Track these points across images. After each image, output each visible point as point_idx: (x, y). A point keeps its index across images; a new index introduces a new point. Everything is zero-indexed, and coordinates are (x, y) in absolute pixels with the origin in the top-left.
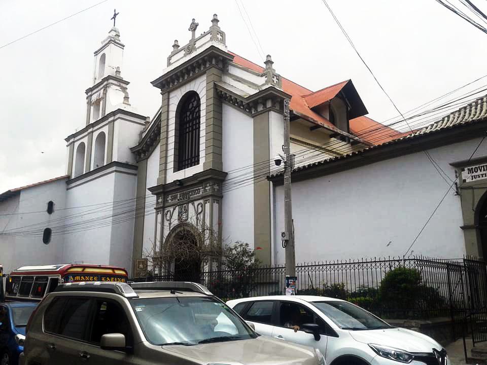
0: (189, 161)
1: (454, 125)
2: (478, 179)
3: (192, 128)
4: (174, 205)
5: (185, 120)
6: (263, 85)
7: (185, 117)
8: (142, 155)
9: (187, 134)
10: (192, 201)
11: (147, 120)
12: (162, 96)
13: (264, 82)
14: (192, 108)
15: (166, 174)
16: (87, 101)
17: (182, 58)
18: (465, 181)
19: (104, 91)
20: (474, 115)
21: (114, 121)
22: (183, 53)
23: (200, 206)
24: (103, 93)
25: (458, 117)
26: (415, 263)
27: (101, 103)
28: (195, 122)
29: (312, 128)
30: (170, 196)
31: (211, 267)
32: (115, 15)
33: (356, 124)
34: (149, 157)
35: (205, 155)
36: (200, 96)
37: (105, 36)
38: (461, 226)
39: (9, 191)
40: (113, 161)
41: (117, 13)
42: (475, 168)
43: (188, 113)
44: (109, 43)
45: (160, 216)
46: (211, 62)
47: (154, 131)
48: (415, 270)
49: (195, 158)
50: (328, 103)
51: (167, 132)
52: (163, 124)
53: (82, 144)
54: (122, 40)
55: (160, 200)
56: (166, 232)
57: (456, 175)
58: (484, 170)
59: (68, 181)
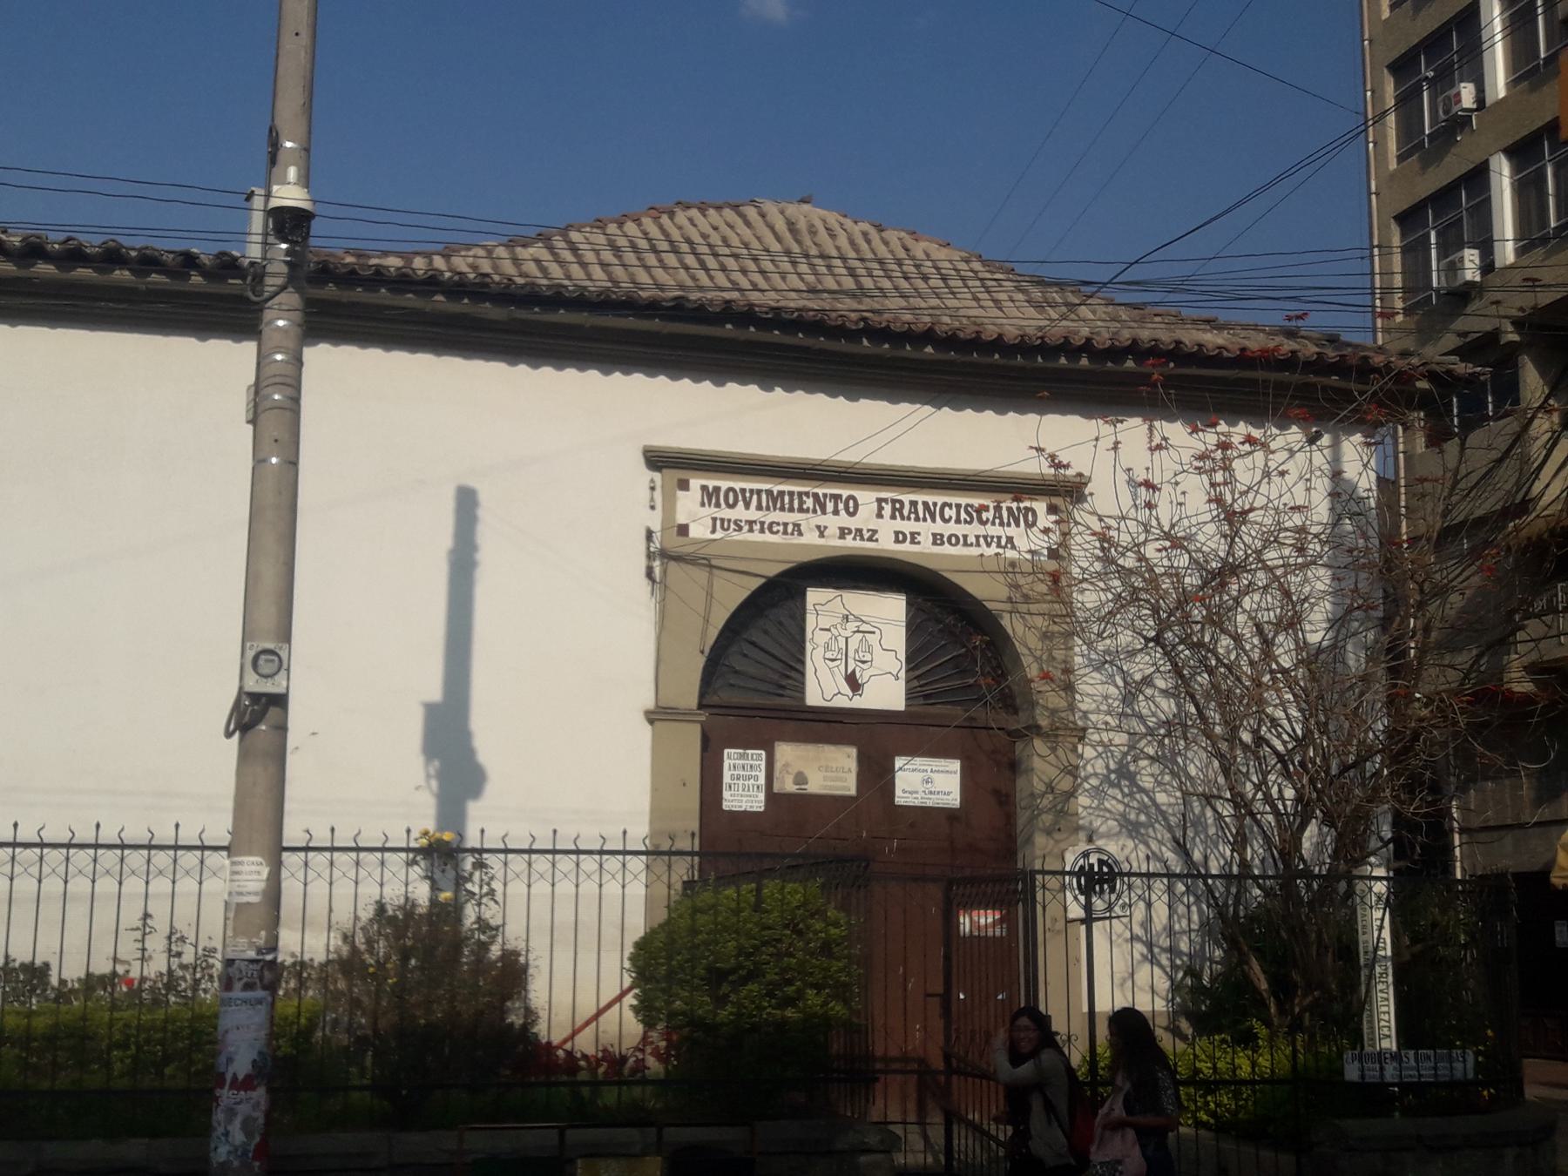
18: (683, 530)
57: (652, 499)
58: (759, 507)
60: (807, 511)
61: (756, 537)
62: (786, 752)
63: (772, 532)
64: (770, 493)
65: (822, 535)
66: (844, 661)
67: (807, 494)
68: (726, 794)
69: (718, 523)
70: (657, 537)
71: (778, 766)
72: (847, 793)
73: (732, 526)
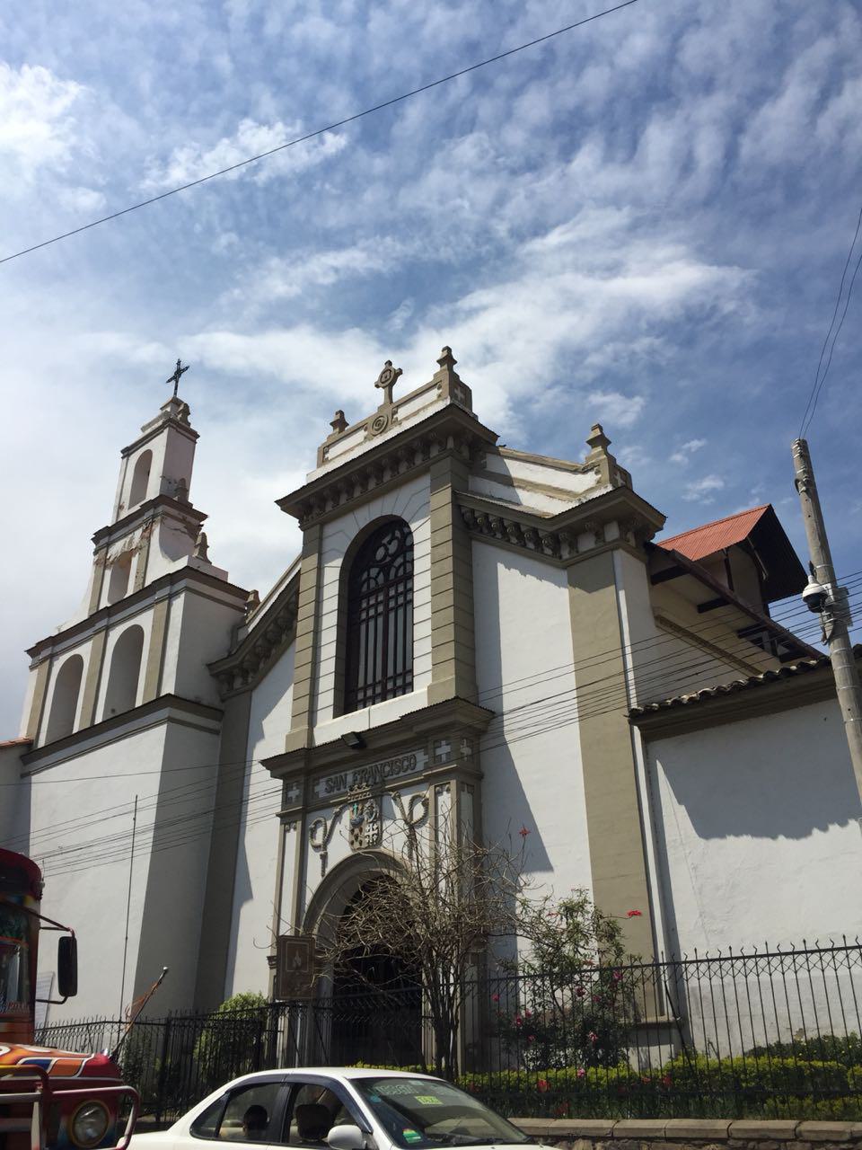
0: (378, 690)
3: (386, 605)
5: (364, 589)
6: (591, 490)
7: (364, 582)
8: (238, 683)
11: (251, 598)
12: (302, 533)
13: (593, 484)
15: (312, 723)
16: (96, 558)
19: (144, 531)
22: (362, 434)
24: (142, 537)
27: (135, 561)
29: (702, 608)
34: (255, 687)
35: (430, 667)
37: (151, 411)
40: (163, 694)
41: (182, 367)
43: (374, 572)
45: (293, 837)
46: (443, 444)
47: (276, 620)
49: (394, 678)
50: (725, 557)
51: (318, 616)
52: (306, 597)
54: (195, 422)
55: (294, 793)
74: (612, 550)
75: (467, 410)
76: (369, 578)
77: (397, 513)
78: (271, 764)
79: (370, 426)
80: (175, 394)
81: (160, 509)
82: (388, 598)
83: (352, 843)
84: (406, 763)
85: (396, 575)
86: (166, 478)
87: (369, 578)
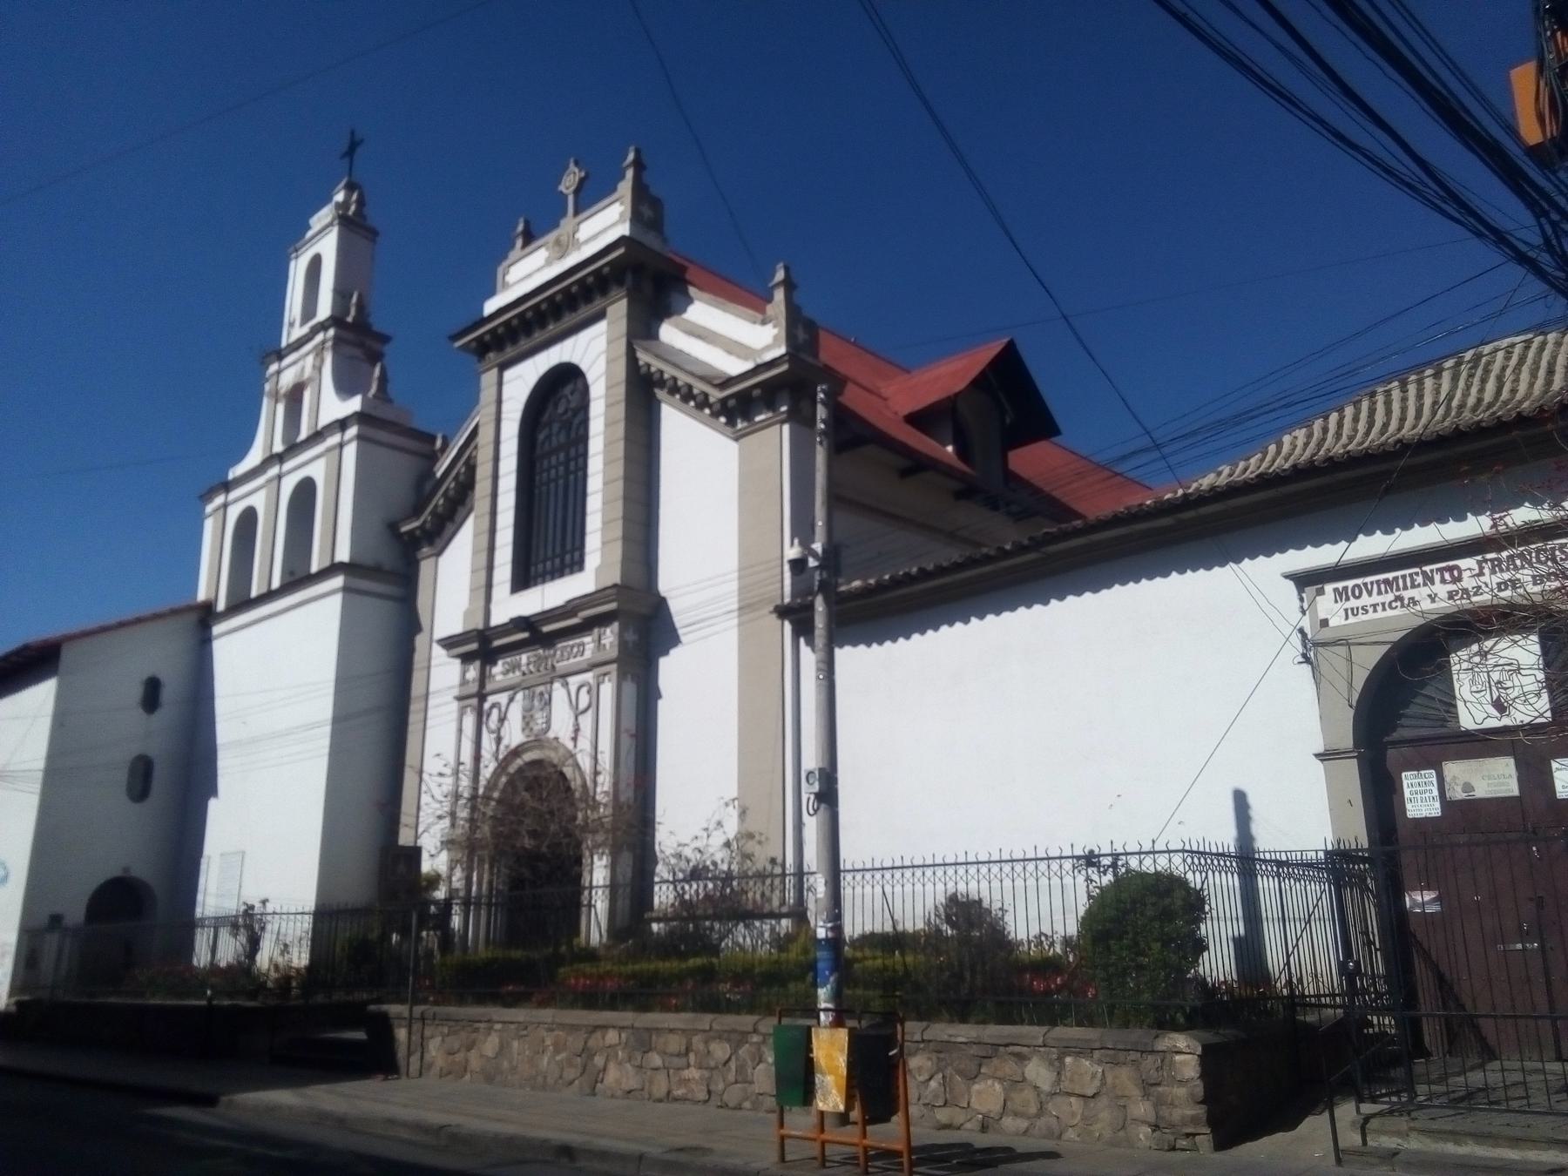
0: (557, 561)
1: (1294, 466)
2: (1365, 618)
4: (513, 688)
6: (768, 348)
7: (543, 443)
9: (552, 485)
10: (564, 676)
14: (566, 412)
17: (539, 270)
18: (1325, 623)
20: (1351, 439)
21: (341, 446)
23: (584, 690)
24: (314, 366)
25: (1306, 445)
26: (1184, 861)
27: (307, 396)
28: (573, 452)
29: (905, 473)
30: (500, 663)
31: (613, 867)
32: (353, 146)
33: (1029, 461)
36: (590, 377)
38: (1317, 752)
39: (26, 648)
42: (1354, 586)
43: (556, 427)
44: (331, 224)
45: (469, 721)
48: (1181, 883)
53: (249, 517)
54: (374, 218)
56: (487, 772)
57: (1302, 607)
58: (1380, 593)
59: (206, 615)
60: (1419, 585)
61: (1380, 614)
62: (1452, 769)
63: (1391, 607)
64: (1386, 582)
65: (1433, 601)
66: (1488, 691)
67: (1417, 574)
68: (1409, 806)
69: (1350, 612)
70: (1308, 630)
71: (1448, 779)
72: (1511, 794)
73: (1360, 611)
74: (782, 422)
75: (650, 240)
76: (549, 437)
77: (575, 360)
78: (449, 643)
79: (551, 245)
80: (350, 175)
81: (331, 332)
82: (568, 460)
83: (523, 730)
84: (575, 650)
85: (577, 433)
86: (341, 294)
87: (549, 437)
